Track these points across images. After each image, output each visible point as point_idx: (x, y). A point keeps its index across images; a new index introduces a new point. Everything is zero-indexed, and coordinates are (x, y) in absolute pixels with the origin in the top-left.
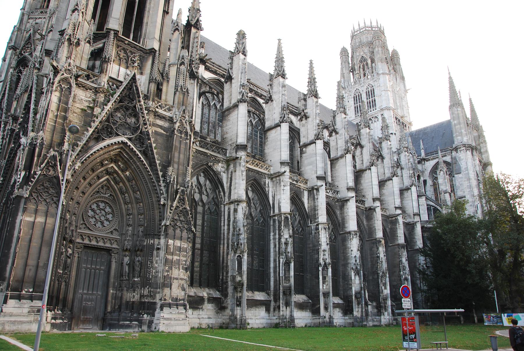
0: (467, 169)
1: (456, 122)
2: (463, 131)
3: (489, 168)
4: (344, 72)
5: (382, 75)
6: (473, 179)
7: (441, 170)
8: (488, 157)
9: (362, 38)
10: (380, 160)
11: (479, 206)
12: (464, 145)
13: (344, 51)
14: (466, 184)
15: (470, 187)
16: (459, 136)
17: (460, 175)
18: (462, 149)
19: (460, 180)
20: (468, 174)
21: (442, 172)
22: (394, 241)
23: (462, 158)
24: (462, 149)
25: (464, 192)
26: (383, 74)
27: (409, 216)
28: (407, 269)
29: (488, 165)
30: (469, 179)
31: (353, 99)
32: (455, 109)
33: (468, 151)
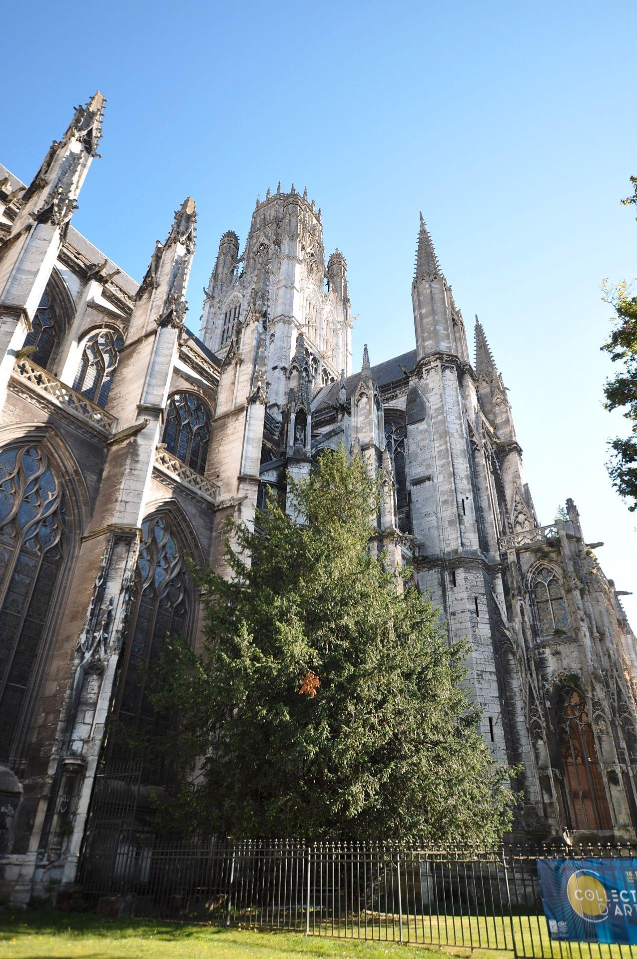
0: (441, 410)
1: (424, 311)
2: (440, 328)
3: (513, 456)
4: (220, 270)
5: (286, 260)
6: (456, 436)
7: (362, 394)
8: (512, 433)
9: (268, 214)
10: (146, 296)
11: (469, 504)
12: (439, 355)
13: (231, 238)
14: (438, 446)
15: (448, 453)
16: (429, 339)
17: (422, 426)
18: (433, 364)
19: (419, 438)
20: (444, 420)
21: (364, 400)
22: (103, 518)
23: (431, 386)
24: (433, 364)
25: (428, 466)
26: (289, 257)
27: (228, 485)
28: (117, 625)
29: (511, 450)
30: (445, 434)
31: (223, 316)
32: (425, 285)
33: (448, 371)
